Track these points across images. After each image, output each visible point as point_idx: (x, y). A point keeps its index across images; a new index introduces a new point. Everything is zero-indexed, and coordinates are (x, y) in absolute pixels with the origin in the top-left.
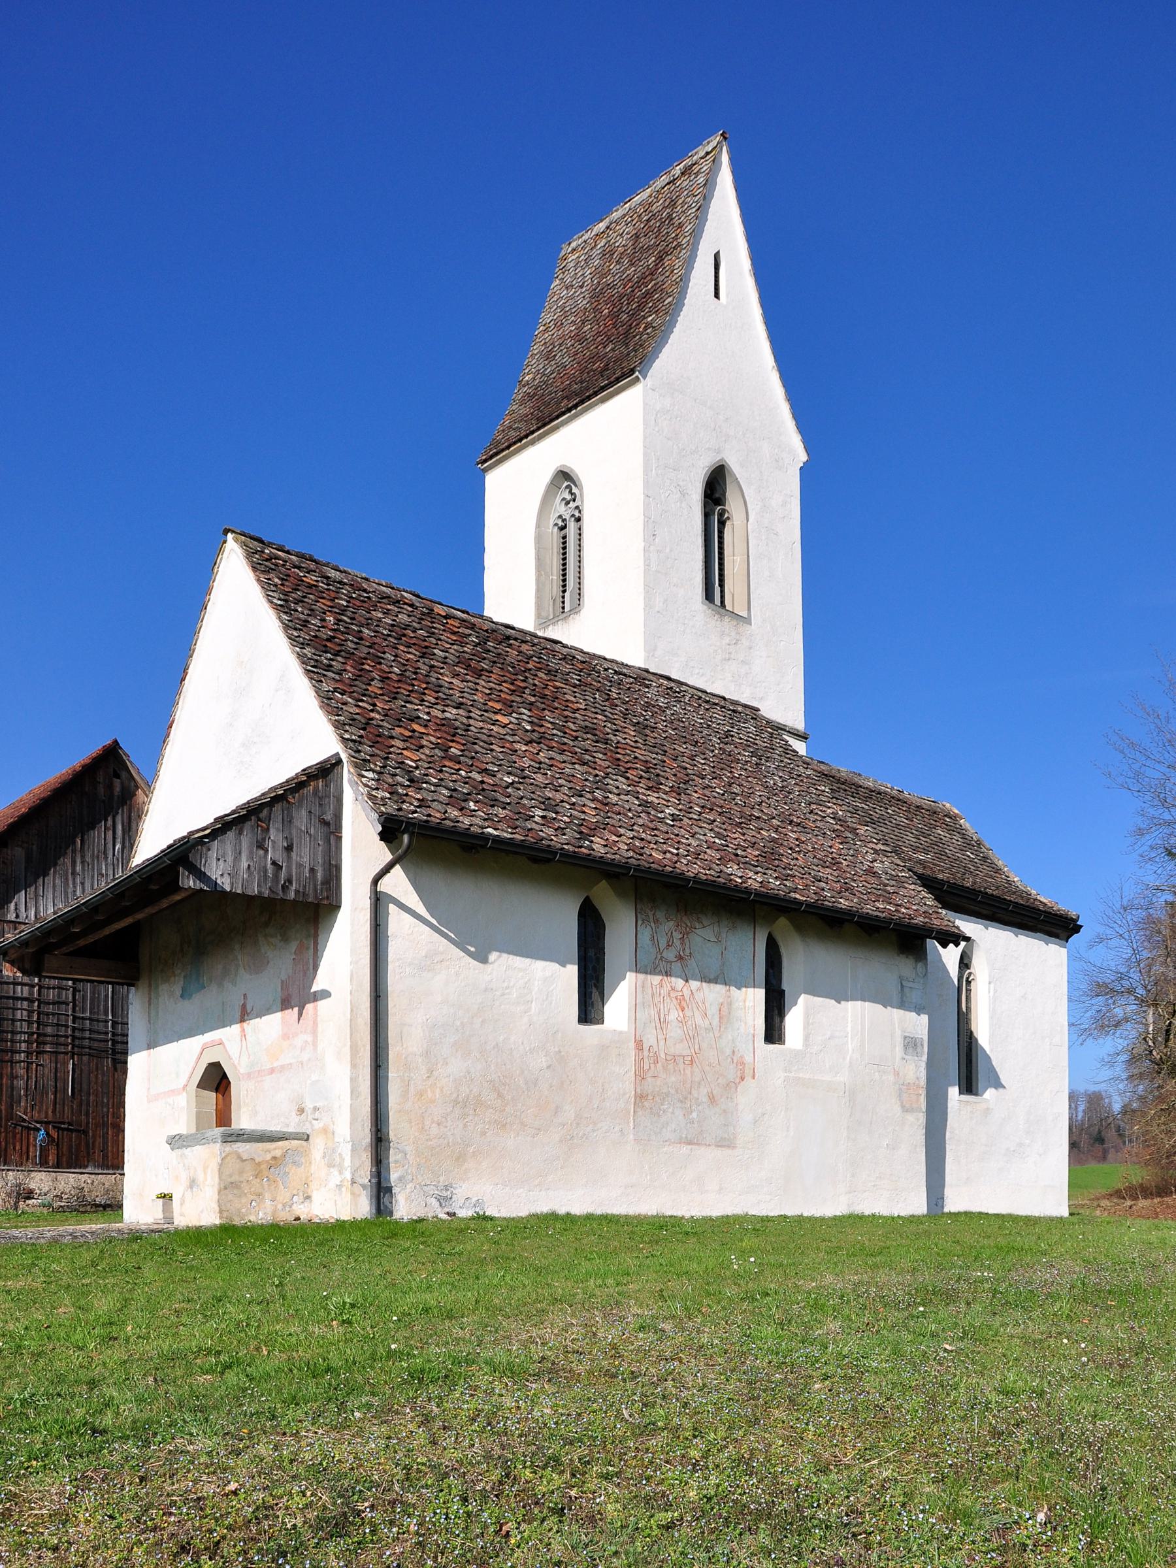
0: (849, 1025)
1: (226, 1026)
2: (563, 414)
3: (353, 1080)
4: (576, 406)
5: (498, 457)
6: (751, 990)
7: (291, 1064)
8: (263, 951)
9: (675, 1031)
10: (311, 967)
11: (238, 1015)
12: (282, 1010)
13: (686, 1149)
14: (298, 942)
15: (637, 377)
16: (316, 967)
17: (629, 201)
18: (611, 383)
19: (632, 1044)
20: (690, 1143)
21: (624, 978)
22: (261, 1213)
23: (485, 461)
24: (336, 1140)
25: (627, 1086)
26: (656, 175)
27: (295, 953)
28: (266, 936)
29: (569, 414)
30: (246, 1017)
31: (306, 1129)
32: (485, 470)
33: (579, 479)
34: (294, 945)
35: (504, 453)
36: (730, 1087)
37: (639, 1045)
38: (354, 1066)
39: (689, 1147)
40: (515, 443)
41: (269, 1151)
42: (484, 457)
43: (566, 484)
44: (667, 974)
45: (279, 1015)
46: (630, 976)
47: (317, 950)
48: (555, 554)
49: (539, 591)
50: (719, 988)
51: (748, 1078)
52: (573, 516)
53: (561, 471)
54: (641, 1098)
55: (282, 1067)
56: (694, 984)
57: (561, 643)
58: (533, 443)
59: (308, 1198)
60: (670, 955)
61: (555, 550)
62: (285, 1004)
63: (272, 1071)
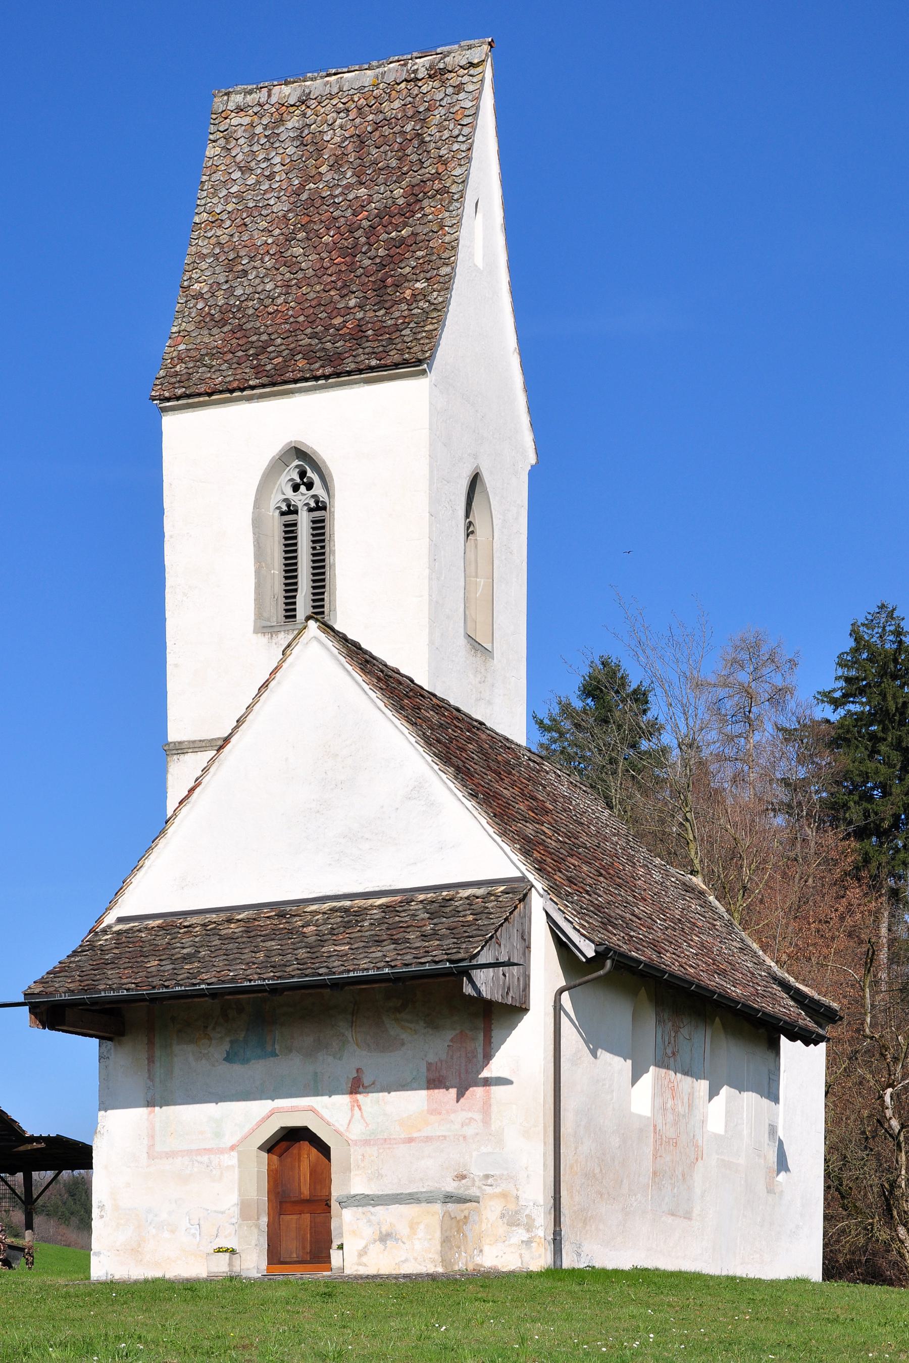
0: (745, 1113)
1: (322, 1095)
2: (306, 380)
3: (545, 1154)
4: (326, 377)
5: (190, 401)
6: (703, 1081)
7: (445, 1137)
8: (392, 1033)
9: (670, 1117)
10: (480, 1056)
11: (347, 1085)
12: (428, 1088)
13: (670, 1219)
14: (458, 1032)
15: (425, 370)
16: (488, 1057)
17: (335, 74)
18: (386, 366)
19: (652, 1128)
20: (673, 1215)
21: (647, 1071)
22: (461, 1264)
23: (168, 399)
24: (522, 1202)
25: (647, 1165)
26: (384, 57)
27: (452, 1040)
28: (396, 1020)
29: (314, 383)
30: (361, 1089)
31: (474, 1192)
32: (165, 410)
33: (326, 466)
34: (449, 1034)
35: (201, 399)
36: (692, 1165)
37: (655, 1126)
38: (545, 1143)
39: (672, 1217)
40: (221, 392)
41: (462, 1211)
42: (167, 394)
43: (297, 462)
44: (668, 1068)
45: (424, 1093)
46: (652, 1068)
47: (490, 1043)
48: (276, 543)
49: (259, 586)
50: (689, 1079)
51: (700, 1159)
52: (307, 504)
53: (295, 448)
54: (655, 1173)
55: (427, 1137)
56: (679, 1075)
57: (485, 725)
58: (249, 399)
59: (481, 1251)
60: (669, 1051)
61: (276, 538)
62: (435, 1082)
63: (410, 1140)
